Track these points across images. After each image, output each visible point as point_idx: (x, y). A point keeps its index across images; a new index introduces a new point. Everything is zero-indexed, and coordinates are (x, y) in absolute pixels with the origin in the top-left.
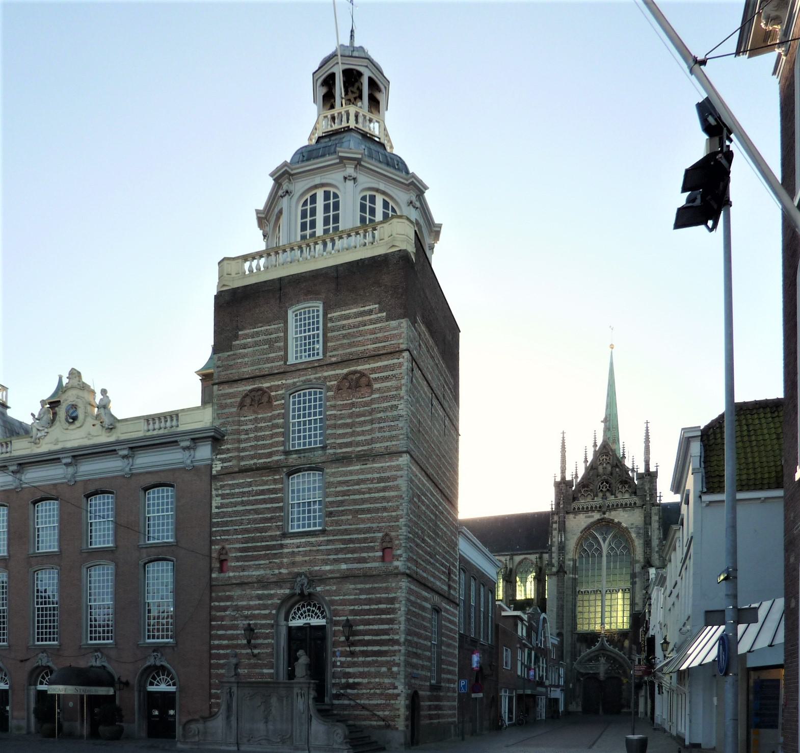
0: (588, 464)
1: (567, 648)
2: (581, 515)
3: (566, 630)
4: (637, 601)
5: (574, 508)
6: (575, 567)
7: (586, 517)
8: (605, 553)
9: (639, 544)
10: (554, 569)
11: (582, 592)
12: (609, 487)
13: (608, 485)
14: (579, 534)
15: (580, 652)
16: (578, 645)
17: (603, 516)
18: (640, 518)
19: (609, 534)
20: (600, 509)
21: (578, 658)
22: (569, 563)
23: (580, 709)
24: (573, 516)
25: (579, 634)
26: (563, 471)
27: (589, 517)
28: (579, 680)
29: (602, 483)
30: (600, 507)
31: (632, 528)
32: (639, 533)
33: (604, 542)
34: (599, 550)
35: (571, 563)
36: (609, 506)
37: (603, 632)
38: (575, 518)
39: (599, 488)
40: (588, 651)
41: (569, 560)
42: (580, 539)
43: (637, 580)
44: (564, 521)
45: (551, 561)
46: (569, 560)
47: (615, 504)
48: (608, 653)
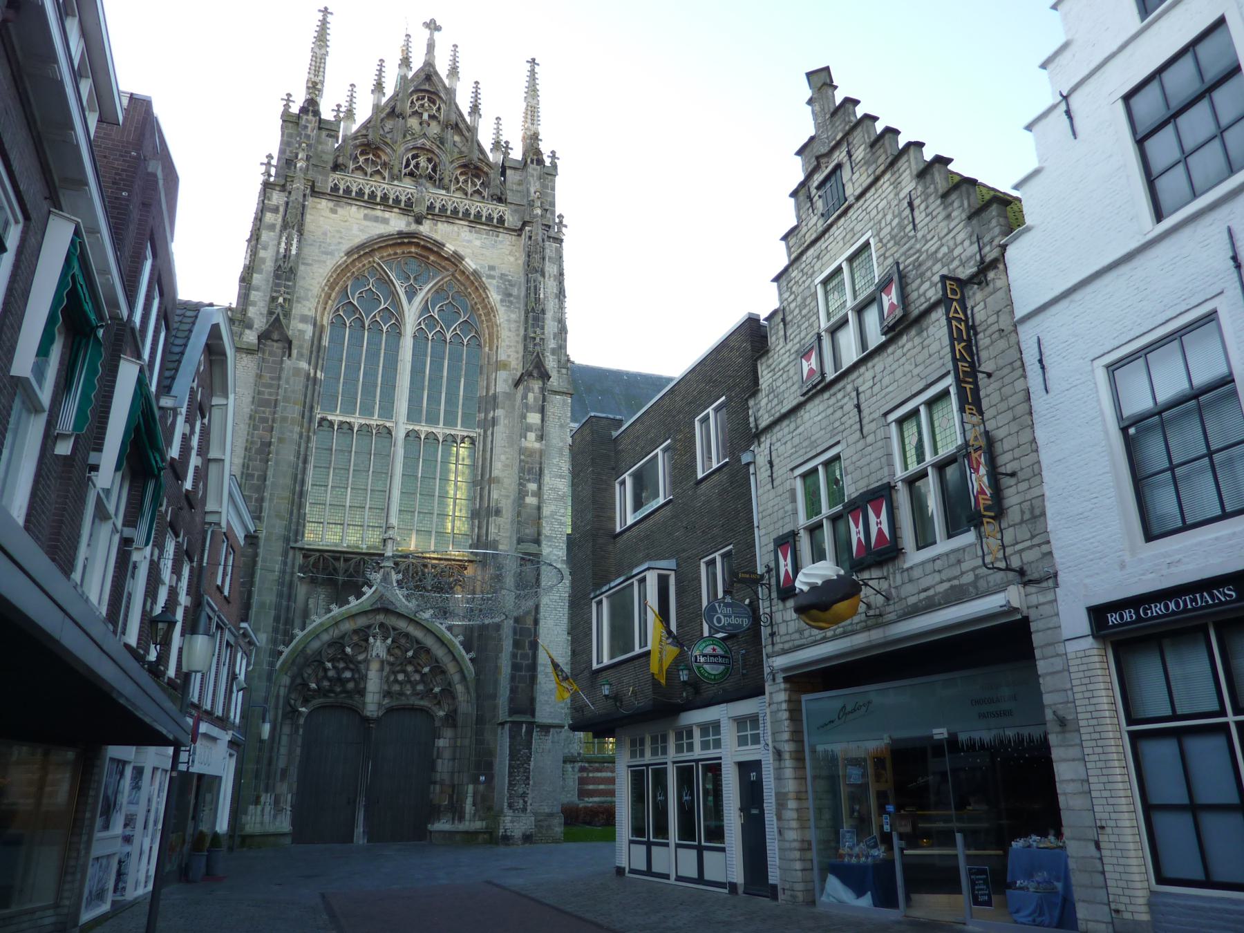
0: (384, 100)
1: (265, 594)
2: (354, 209)
3: (272, 529)
4: (495, 473)
5: (335, 188)
6: (316, 348)
7: (366, 217)
8: (409, 328)
9: (509, 321)
10: (251, 337)
11: (331, 424)
12: (434, 169)
13: (430, 166)
14: (339, 257)
15: (306, 615)
16: (302, 590)
17: (414, 227)
18: (512, 259)
19: (426, 283)
20: (407, 208)
21: (300, 635)
22: (301, 326)
23: (284, 824)
24: (331, 204)
25: (307, 553)
26: (314, 87)
27: (376, 219)
28: (292, 713)
29: (414, 157)
30: (409, 203)
31: (492, 277)
32: (510, 295)
33: (410, 301)
34: (395, 315)
35: (309, 330)
36: (431, 207)
37: (389, 553)
38: (334, 211)
39: (407, 165)
40: (336, 610)
41: (304, 319)
42: (342, 271)
43: (500, 412)
44: (304, 206)
45: (244, 312)
46: (304, 319)
47: (450, 208)
48: (402, 624)
